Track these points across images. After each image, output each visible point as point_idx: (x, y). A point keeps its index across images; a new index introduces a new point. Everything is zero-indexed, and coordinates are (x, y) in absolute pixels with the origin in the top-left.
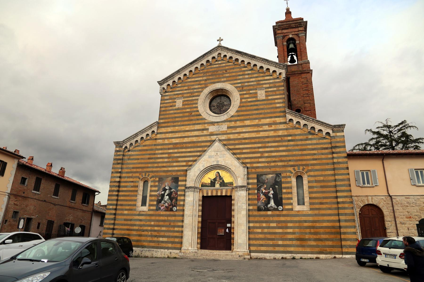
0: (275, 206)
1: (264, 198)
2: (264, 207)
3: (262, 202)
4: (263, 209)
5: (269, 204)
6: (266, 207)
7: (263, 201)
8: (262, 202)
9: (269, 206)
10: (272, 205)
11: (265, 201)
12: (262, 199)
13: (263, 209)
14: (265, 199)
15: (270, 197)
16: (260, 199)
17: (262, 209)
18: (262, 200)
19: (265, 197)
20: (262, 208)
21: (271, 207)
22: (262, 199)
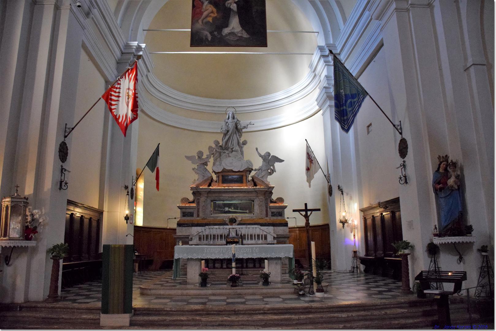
0: (244, 32)
1: (212, 12)
2: (211, 33)
3: (205, 21)
4: (210, 39)
5: (227, 26)
6: (216, 33)
7: (210, 19)
8: (205, 21)
9: (226, 31)
10: (233, 28)
11: (214, 19)
12: (205, 14)
13: (210, 39)
14: (216, 15)
15: (230, 9)
16: (201, 13)
17: (207, 39)
18: (207, 17)
19: (215, 10)
20: (206, 35)
21: (232, 33)
22: (205, 14)
